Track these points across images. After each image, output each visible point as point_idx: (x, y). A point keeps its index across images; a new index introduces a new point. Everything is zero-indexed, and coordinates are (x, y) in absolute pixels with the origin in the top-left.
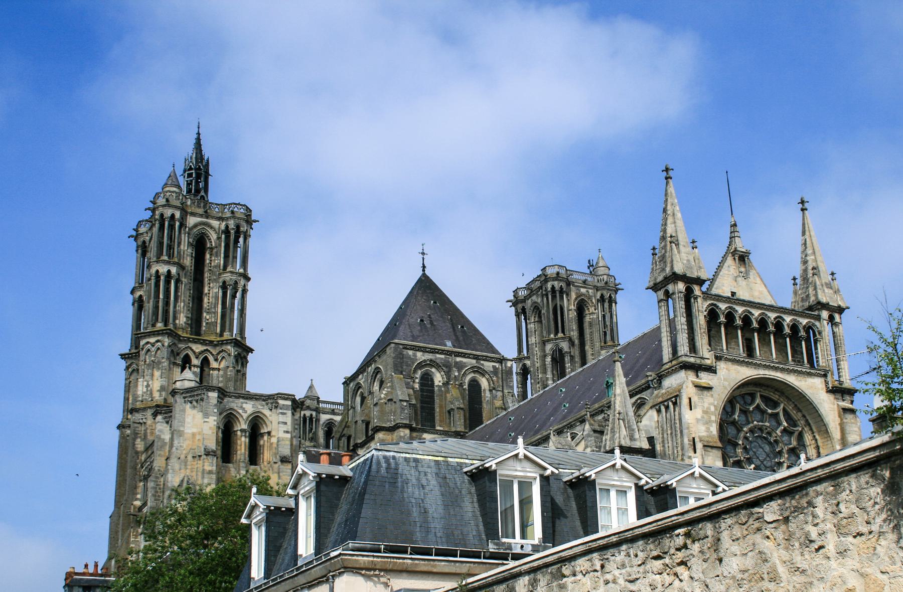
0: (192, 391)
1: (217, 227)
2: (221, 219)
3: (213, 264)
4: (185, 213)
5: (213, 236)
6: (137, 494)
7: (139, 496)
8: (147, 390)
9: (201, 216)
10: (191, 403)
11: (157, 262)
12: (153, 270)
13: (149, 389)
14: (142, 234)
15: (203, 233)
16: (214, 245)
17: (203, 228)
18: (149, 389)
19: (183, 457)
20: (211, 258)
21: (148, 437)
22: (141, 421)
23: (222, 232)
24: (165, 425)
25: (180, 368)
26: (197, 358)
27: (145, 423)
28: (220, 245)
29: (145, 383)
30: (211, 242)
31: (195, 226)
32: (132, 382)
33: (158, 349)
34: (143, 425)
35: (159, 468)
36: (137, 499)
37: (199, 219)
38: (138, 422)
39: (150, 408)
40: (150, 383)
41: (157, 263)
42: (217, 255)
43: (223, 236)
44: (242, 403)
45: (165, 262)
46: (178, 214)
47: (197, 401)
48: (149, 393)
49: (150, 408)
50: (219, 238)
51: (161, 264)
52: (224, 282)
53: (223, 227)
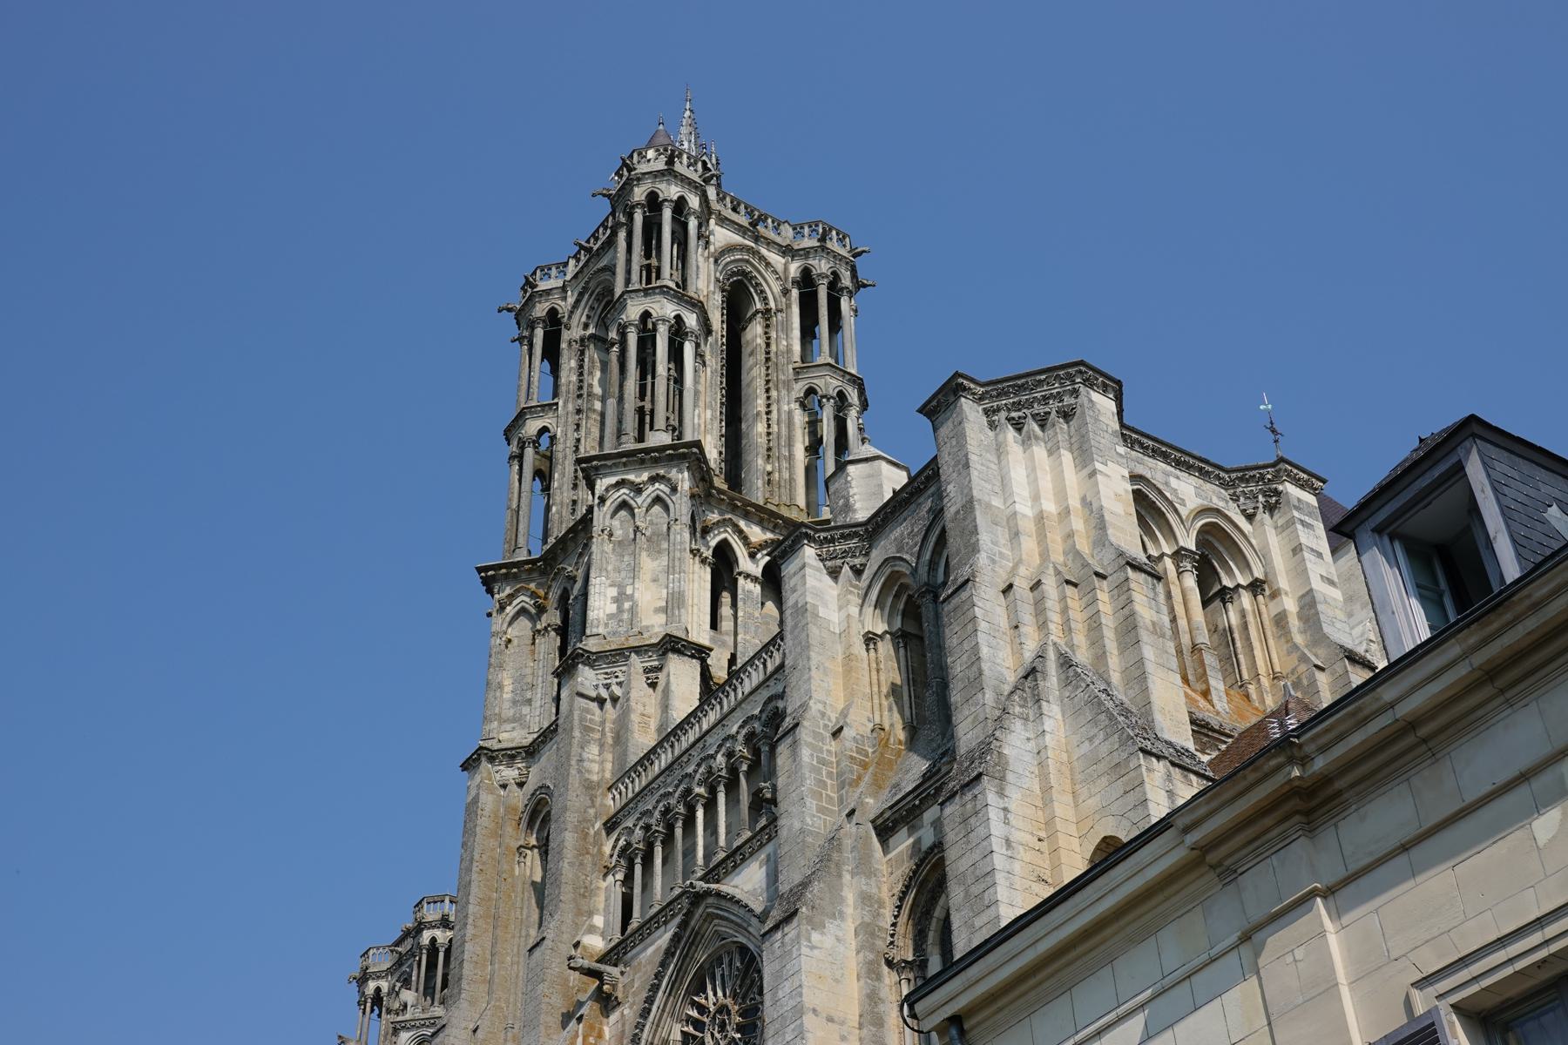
0: (1022, 388)
1: (780, 268)
2: (787, 251)
3: (773, 348)
4: (706, 211)
5: (773, 287)
6: (590, 914)
7: (598, 921)
8: (620, 610)
9: (740, 229)
10: (1018, 426)
11: (647, 292)
12: (633, 311)
13: (627, 605)
14: (548, 292)
15: (744, 273)
16: (772, 305)
17: (747, 261)
18: (627, 605)
19: (1022, 585)
20: (766, 333)
21: (636, 735)
22: (604, 694)
23: (793, 283)
24: (828, 580)
25: (709, 570)
26: (752, 556)
27: (615, 700)
28: (789, 306)
29: (613, 592)
30: (766, 298)
31: (730, 249)
32: (515, 642)
33: (658, 500)
34: (608, 705)
35: (820, 707)
36: (592, 930)
37: (737, 239)
38: (593, 694)
39: (638, 650)
40: (629, 591)
41: (646, 295)
42: (787, 329)
43: (795, 293)
44: (1167, 474)
45: (664, 291)
46: (694, 202)
47: (1043, 421)
48: (626, 616)
49: (638, 650)
50: (786, 292)
51: (658, 298)
52: (811, 391)
53: (794, 268)
